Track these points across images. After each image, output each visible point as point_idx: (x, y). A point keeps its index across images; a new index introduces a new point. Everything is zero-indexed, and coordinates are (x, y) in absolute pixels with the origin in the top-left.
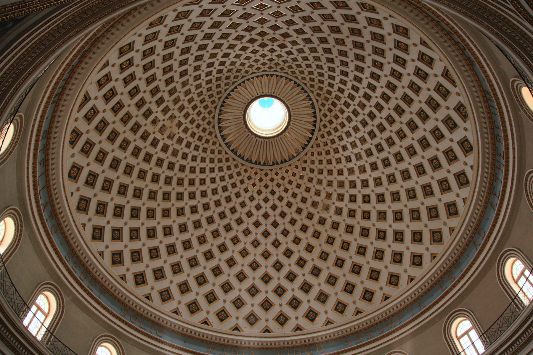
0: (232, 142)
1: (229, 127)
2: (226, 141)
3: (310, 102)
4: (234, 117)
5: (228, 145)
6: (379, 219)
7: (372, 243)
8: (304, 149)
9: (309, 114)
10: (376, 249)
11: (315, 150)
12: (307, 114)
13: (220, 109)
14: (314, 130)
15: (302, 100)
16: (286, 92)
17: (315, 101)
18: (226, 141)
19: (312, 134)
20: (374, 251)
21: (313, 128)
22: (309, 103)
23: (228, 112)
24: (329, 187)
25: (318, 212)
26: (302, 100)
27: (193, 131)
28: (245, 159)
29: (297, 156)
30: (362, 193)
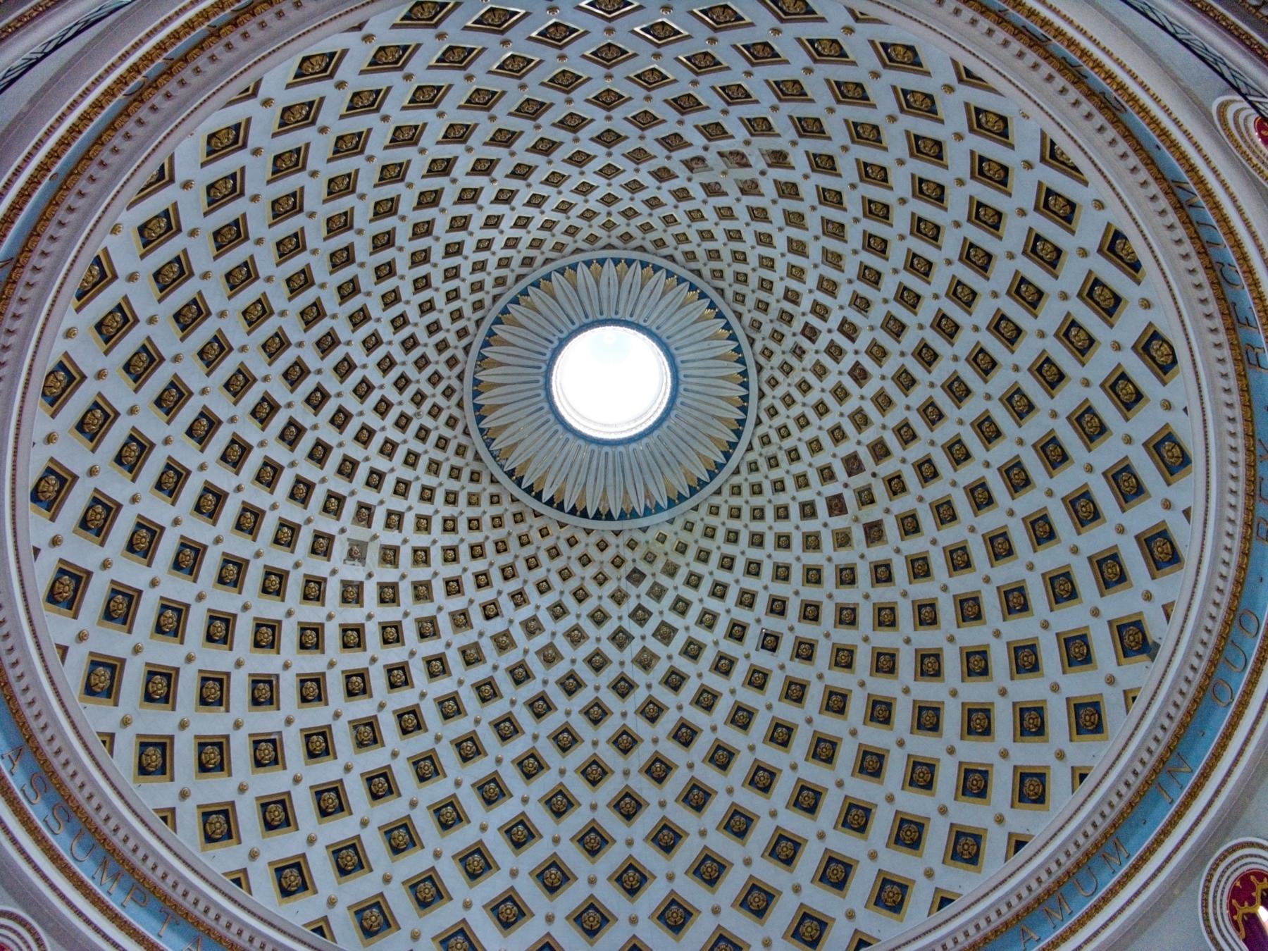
6: (355, 727)
8: (510, 474)
10: (276, 737)
19: (550, 503)
29: (491, 453)
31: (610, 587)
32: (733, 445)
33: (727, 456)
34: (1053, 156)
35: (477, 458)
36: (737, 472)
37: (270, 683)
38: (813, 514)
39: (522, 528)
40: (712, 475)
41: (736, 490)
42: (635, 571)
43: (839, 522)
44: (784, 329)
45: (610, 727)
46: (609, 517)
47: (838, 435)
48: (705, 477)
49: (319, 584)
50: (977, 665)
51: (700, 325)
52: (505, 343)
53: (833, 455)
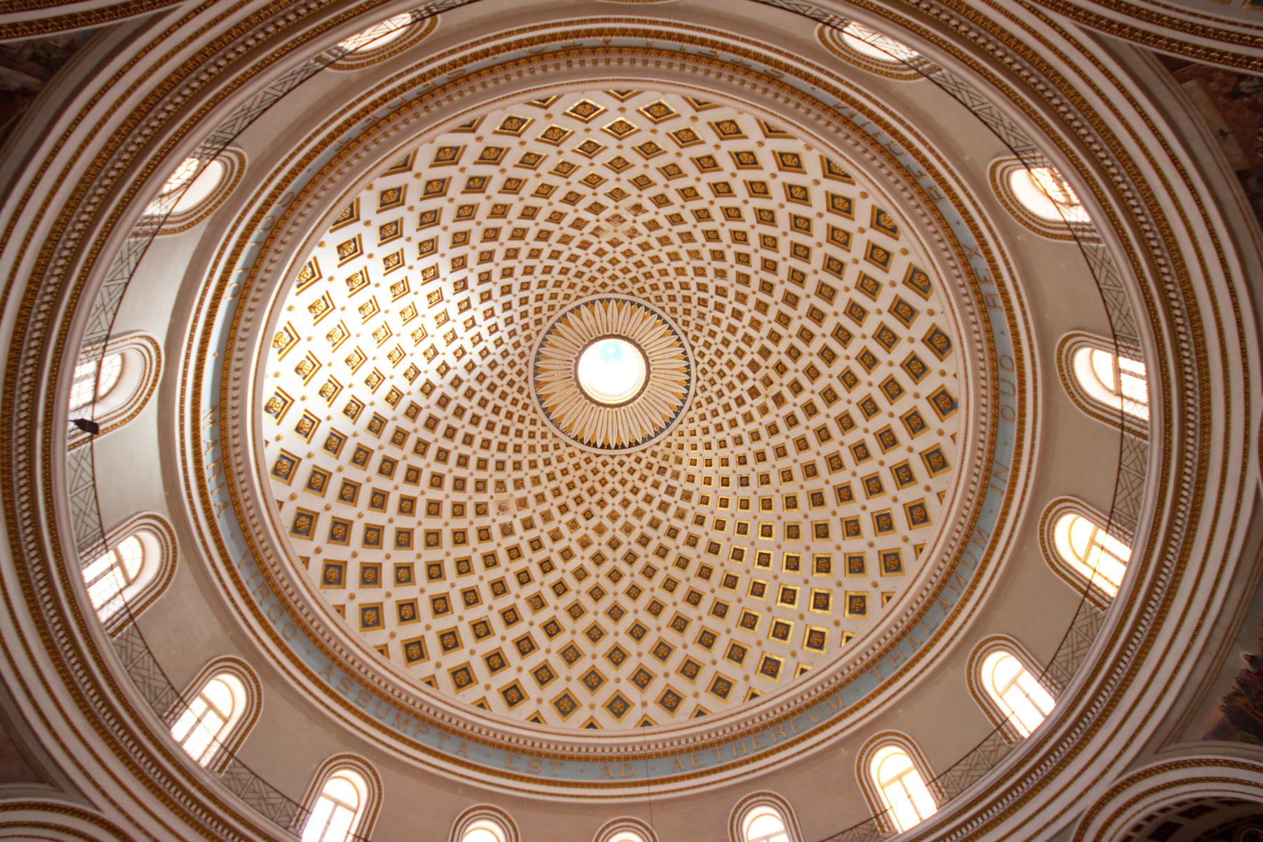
2: (570, 315)
8: (576, 439)
19: (602, 447)
31: (649, 481)
32: (688, 381)
33: (688, 388)
34: (770, 131)
35: (555, 436)
36: (696, 395)
38: (743, 402)
39: (592, 466)
40: (684, 402)
41: (699, 405)
42: (660, 468)
43: (758, 401)
44: (688, 306)
45: (672, 557)
46: (637, 444)
47: (740, 353)
50: (861, 452)
51: (646, 322)
52: (545, 370)
53: (741, 365)
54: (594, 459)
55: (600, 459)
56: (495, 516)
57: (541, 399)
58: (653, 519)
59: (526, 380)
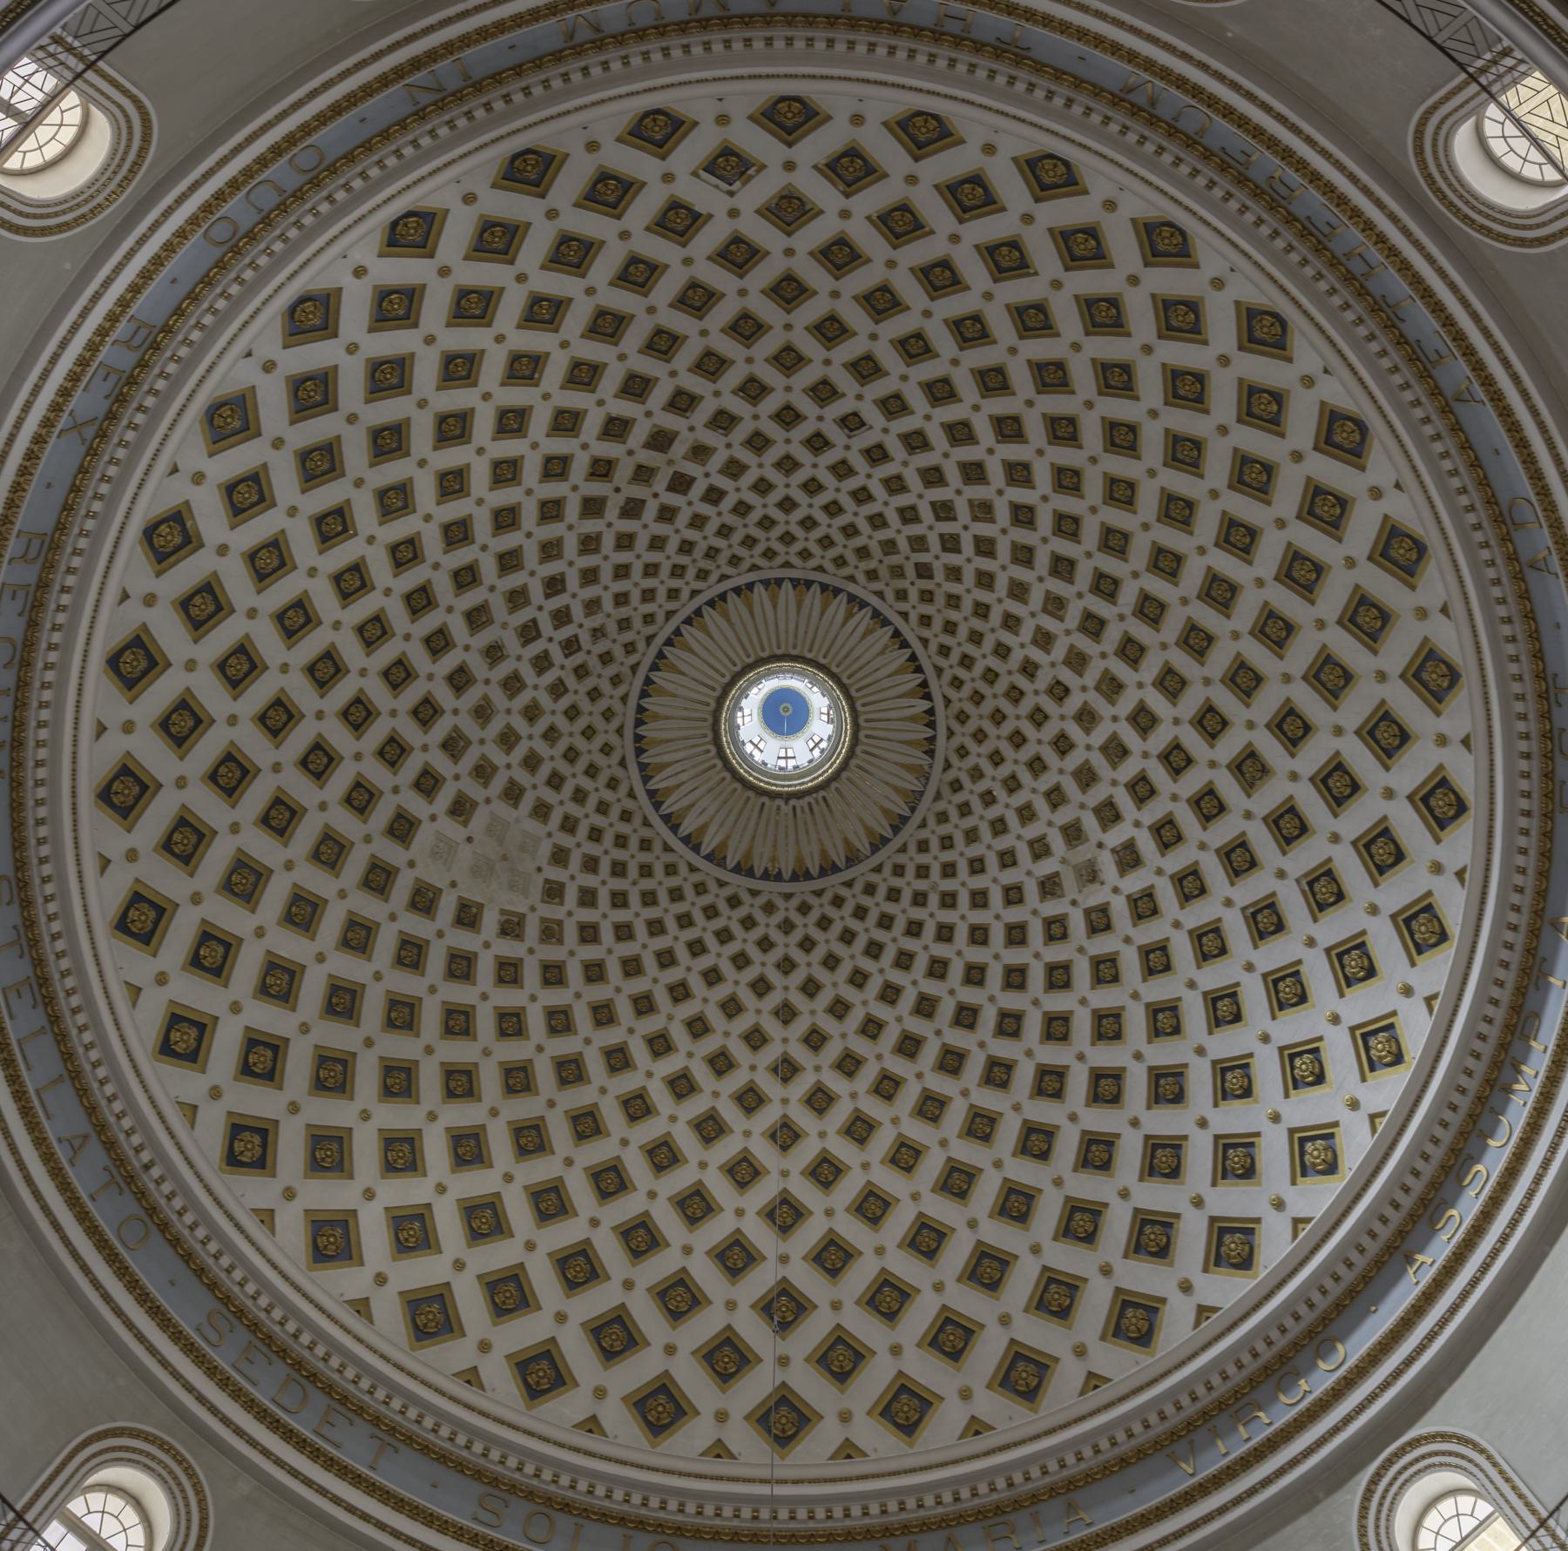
0: (723, 845)
1: (693, 805)
3: (867, 612)
4: (692, 772)
5: (716, 858)
6: (1251, 785)
7: (1281, 874)
8: (931, 753)
9: (886, 647)
10: (1304, 882)
11: (963, 736)
12: (882, 653)
13: (639, 764)
14: (924, 684)
15: (843, 625)
16: (792, 626)
17: (874, 601)
18: (705, 850)
19: (928, 697)
20: (1303, 892)
21: (919, 678)
22: (863, 618)
23: (668, 765)
24: (1061, 809)
25: (1074, 903)
26: (843, 625)
27: (585, 855)
28: (787, 875)
30: (1156, 753)
35: (938, 796)
37: (1254, 915)
46: (897, 634)
48: (787, 586)
49: (1135, 901)
54: (956, 706)
55: (952, 694)
56: (1107, 888)
57: (878, 843)
58: (1016, 560)
59: (849, 884)
